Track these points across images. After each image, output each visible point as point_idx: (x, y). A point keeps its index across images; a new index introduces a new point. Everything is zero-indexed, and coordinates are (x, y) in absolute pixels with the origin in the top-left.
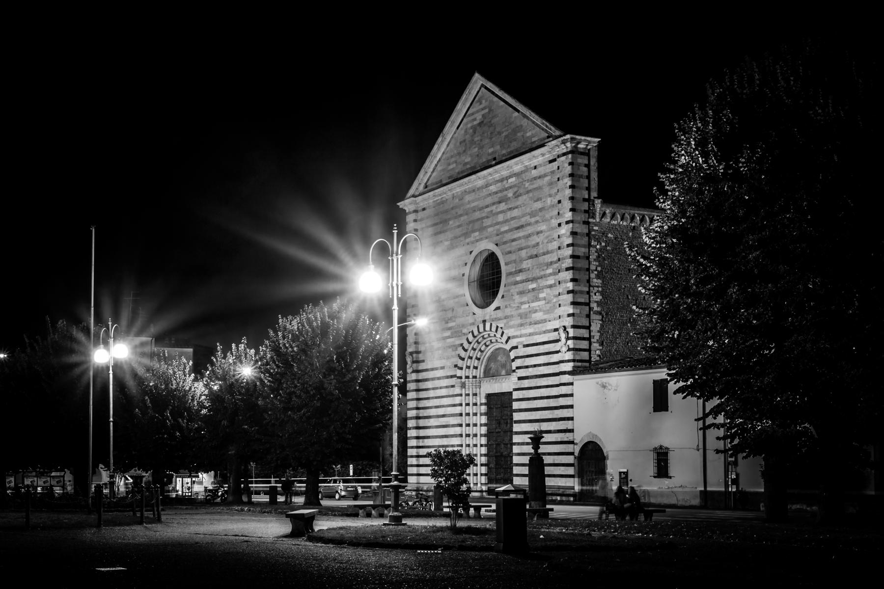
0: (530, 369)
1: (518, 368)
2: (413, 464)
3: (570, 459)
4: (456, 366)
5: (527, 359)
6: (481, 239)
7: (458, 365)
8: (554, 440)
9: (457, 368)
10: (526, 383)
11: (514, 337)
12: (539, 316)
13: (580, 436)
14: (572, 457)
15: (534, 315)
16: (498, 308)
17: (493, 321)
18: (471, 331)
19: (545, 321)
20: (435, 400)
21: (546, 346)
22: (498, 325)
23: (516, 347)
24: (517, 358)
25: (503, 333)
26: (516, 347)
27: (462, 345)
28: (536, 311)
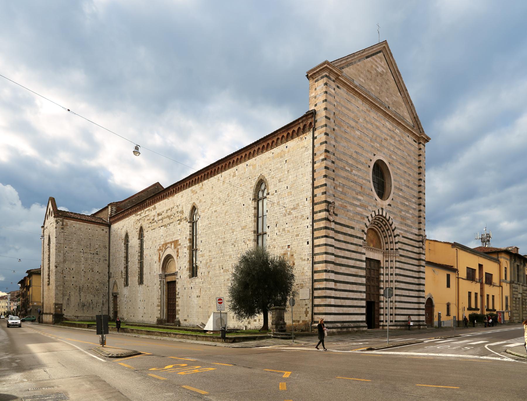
1: (400, 248)
4: (363, 231)
7: (365, 231)
10: (403, 259)
11: (399, 229)
12: (409, 222)
13: (426, 295)
15: (407, 220)
21: (412, 241)
22: (390, 216)
24: (399, 242)
25: (392, 223)
27: (368, 217)
28: (408, 219)
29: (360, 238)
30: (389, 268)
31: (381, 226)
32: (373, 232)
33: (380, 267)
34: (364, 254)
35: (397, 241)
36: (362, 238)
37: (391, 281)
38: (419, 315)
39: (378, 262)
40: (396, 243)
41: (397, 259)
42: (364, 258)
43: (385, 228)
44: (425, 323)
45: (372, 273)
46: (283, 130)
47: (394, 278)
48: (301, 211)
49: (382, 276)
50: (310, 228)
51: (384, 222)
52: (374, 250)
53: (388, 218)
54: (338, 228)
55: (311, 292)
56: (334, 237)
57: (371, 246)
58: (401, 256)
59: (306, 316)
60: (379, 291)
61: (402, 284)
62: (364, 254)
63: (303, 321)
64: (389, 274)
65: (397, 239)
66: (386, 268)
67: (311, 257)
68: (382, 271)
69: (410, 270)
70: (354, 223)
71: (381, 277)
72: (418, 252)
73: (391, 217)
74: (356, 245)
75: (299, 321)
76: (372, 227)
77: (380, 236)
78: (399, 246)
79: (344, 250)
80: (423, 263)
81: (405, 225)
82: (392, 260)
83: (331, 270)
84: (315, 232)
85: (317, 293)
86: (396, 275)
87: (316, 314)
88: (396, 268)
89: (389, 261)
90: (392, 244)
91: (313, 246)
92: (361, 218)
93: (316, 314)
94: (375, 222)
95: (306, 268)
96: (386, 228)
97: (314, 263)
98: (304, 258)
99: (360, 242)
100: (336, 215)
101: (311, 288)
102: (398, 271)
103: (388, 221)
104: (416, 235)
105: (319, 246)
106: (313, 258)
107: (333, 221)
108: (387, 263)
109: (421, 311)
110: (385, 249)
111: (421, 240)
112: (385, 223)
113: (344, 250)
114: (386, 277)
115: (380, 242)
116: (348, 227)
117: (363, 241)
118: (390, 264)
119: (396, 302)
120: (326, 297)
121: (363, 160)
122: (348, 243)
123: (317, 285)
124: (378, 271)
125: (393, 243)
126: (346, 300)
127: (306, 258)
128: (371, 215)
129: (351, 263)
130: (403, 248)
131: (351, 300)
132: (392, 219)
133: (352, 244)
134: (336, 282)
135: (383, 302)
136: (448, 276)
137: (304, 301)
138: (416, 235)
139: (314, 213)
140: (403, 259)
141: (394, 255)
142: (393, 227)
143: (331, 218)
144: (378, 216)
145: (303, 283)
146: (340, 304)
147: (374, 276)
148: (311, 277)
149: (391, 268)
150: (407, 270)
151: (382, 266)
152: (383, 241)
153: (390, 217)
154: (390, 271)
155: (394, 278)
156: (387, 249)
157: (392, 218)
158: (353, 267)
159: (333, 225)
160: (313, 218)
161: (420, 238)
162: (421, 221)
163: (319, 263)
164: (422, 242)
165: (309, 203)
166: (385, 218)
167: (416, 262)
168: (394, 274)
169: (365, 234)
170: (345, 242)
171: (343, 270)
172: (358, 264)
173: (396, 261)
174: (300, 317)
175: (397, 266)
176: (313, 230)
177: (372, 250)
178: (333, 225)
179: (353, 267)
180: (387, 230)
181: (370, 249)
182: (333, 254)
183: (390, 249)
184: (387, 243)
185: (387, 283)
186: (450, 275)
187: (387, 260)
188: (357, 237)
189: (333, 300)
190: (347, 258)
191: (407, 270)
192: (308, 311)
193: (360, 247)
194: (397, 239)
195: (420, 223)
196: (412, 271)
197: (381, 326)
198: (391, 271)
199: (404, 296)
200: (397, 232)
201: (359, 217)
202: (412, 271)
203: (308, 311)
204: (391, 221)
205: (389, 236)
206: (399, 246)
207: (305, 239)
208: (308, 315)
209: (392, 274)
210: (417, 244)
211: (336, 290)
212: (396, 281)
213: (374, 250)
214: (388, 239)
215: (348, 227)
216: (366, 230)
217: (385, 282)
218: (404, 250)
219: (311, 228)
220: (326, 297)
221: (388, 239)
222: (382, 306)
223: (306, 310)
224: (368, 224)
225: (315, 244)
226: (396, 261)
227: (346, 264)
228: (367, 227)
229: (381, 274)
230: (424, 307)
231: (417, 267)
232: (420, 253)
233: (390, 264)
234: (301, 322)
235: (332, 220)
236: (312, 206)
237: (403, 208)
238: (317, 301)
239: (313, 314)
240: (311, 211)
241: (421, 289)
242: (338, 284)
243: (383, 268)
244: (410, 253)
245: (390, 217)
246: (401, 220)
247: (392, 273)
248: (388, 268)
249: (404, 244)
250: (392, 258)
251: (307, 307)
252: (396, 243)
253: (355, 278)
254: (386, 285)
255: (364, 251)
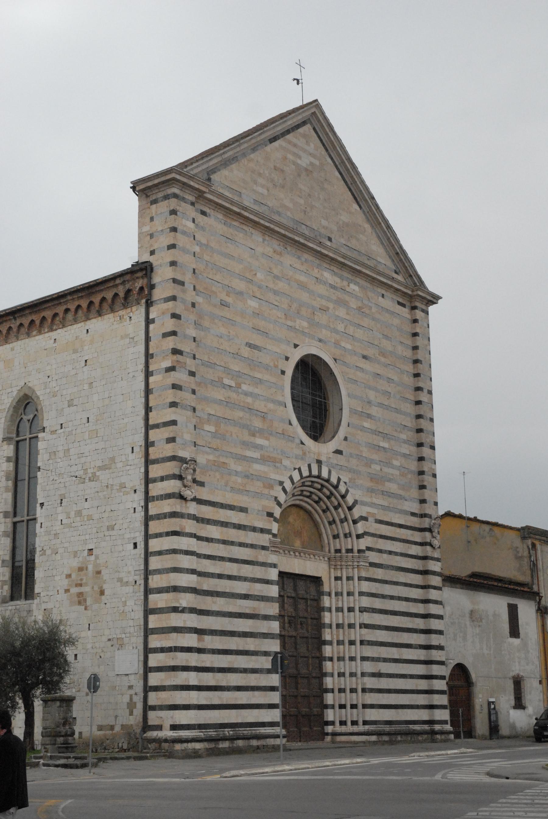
0: (385, 556)
1: (369, 549)
2: (191, 684)
3: (441, 685)
5: (380, 540)
6: (312, 337)
7: (275, 515)
8: (415, 658)
9: (272, 519)
10: (379, 573)
11: (364, 504)
12: (393, 487)
14: (444, 682)
15: (387, 484)
16: (338, 452)
17: (333, 467)
18: (298, 467)
19: (401, 497)
20: (228, 564)
21: (403, 531)
22: (341, 477)
23: (365, 519)
24: (366, 534)
25: (347, 491)
26: (365, 519)
27: (281, 483)
28: (390, 480)
29: (262, 531)
30: (345, 594)
31: (320, 499)
32: (302, 513)
33: (321, 593)
34: (275, 566)
35: (360, 532)
36: (269, 532)
37: (351, 626)
38: (431, 707)
39: (317, 581)
40: (359, 537)
41: (364, 574)
42: (273, 574)
43: (329, 504)
44: (448, 727)
45: (301, 606)
46: (80, 295)
47: (358, 618)
48: (121, 473)
49: (327, 614)
50: (140, 514)
51: (325, 490)
52: (302, 554)
53: (334, 480)
54: (207, 512)
55: (142, 658)
56: (195, 534)
57: (298, 544)
58: (372, 565)
59: (131, 713)
60: (320, 650)
61: (378, 632)
62: (275, 566)
63: (122, 725)
64: (346, 610)
65: (361, 527)
66: (337, 594)
67: (142, 577)
68: (326, 602)
69: (400, 598)
70: (245, 498)
71: (324, 616)
72: (420, 554)
73: (344, 479)
74: (252, 546)
75: (112, 728)
76: (298, 502)
77: (317, 522)
78: (363, 543)
79: (222, 559)
80: (436, 581)
81: (383, 494)
82: (351, 575)
83: (188, 607)
84: (151, 523)
85: (154, 660)
86: (362, 610)
87: (153, 708)
88: (361, 594)
89: (344, 578)
90: (349, 539)
91: (147, 554)
92: (264, 487)
93: (153, 708)
94: (302, 491)
95: (130, 603)
96: (331, 503)
97: (147, 591)
98: (125, 580)
99: (264, 539)
100: (202, 484)
101: (141, 647)
102: (366, 602)
103: (336, 487)
104: (413, 514)
105: (160, 553)
106: (146, 580)
107: (195, 499)
108: (339, 582)
109: (436, 696)
110: (333, 551)
111: (427, 526)
112: (328, 493)
113: (222, 559)
114: (337, 617)
115: (320, 535)
116: (231, 507)
117: (271, 536)
118: (345, 586)
119: (363, 674)
120: (174, 669)
121: (265, 359)
122: (232, 543)
123: (155, 642)
124: (318, 600)
125: (350, 536)
126: (229, 675)
127: (131, 579)
128: (291, 478)
129: (241, 587)
130: (379, 547)
131: (241, 674)
132: (345, 483)
133: (241, 545)
134: (200, 632)
135: (332, 675)
136: (513, 610)
137: (126, 678)
138: (413, 514)
139: (148, 481)
140: (379, 573)
141: (356, 564)
142: (350, 500)
143: (188, 493)
144: (308, 479)
145: (123, 636)
146: (212, 683)
147: (306, 615)
148: (142, 623)
149: (349, 594)
150: (392, 598)
151: (326, 588)
152: (327, 531)
153: (339, 480)
154: (346, 602)
155: (358, 618)
156: (338, 551)
157: (347, 481)
158: (246, 597)
159: (192, 508)
160: (147, 492)
161: (426, 523)
162: (425, 483)
163: (160, 591)
164: (430, 530)
165: (138, 459)
166: (328, 481)
167: (417, 579)
168: (357, 609)
169: (276, 520)
170: (224, 542)
171: (219, 604)
172: (258, 589)
173: (360, 579)
174: (116, 717)
175: (364, 590)
176: (148, 518)
177: (297, 554)
178: (192, 508)
179: (246, 597)
180: (336, 508)
181: (292, 553)
182: (193, 572)
183: (343, 551)
184: (336, 537)
185: (341, 631)
186: (518, 606)
187: (339, 575)
188: (254, 529)
189: (193, 674)
190: (230, 577)
191: (392, 598)
192: (135, 703)
193: (263, 552)
194: (361, 527)
195: (422, 487)
196: (407, 599)
197: (327, 734)
198: (348, 602)
199: (385, 660)
200: (357, 512)
201: (259, 484)
202: (407, 599)
203: (135, 703)
204: (342, 489)
205: (342, 521)
206: (363, 543)
207: (127, 536)
208: (135, 712)
209: (351, 610)
210: (417, 537)
211: (200, 651)
212: (364, 626)
213: (302, 554)
214: (340, 527)
215: (231, 507)
216: (277, 512)
217: (334, 626)
218: (380, 551)
219: (143, 514)
220: (174, 669)
221: (340, 527)
222: (330, 686)
223: (131, 699)
224: (282, 498)
225: (151, 550)
226: (360, 579)
227: (227, 591)
228: (279, 504)
229: (323, 609)
230: (445, 688)
231: (420, 591)
232: (425, 558)
233: (345, 586)
234: (117, 729)
235: (189, 498)
236: (143, 464)
237: (375, 457)
238: (154, 679)
239: (147, 708)
240: (142, 476)
241: (434, 643)
242: (207, 638)
243: (329, 594)
244: (398, 558)
245: (339, 480)
246: (369, 484)
247: (352, 605)
248: (342, 594)
249: (382, 537)
250: (350, 570)
251: (132, 692)
252: (359, 537)
253: (250, 622)
254: (338, 636)
255: (272, 558)
